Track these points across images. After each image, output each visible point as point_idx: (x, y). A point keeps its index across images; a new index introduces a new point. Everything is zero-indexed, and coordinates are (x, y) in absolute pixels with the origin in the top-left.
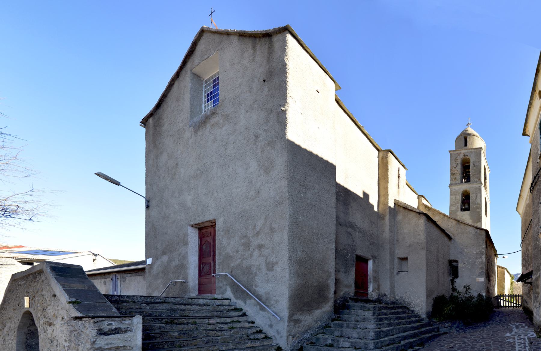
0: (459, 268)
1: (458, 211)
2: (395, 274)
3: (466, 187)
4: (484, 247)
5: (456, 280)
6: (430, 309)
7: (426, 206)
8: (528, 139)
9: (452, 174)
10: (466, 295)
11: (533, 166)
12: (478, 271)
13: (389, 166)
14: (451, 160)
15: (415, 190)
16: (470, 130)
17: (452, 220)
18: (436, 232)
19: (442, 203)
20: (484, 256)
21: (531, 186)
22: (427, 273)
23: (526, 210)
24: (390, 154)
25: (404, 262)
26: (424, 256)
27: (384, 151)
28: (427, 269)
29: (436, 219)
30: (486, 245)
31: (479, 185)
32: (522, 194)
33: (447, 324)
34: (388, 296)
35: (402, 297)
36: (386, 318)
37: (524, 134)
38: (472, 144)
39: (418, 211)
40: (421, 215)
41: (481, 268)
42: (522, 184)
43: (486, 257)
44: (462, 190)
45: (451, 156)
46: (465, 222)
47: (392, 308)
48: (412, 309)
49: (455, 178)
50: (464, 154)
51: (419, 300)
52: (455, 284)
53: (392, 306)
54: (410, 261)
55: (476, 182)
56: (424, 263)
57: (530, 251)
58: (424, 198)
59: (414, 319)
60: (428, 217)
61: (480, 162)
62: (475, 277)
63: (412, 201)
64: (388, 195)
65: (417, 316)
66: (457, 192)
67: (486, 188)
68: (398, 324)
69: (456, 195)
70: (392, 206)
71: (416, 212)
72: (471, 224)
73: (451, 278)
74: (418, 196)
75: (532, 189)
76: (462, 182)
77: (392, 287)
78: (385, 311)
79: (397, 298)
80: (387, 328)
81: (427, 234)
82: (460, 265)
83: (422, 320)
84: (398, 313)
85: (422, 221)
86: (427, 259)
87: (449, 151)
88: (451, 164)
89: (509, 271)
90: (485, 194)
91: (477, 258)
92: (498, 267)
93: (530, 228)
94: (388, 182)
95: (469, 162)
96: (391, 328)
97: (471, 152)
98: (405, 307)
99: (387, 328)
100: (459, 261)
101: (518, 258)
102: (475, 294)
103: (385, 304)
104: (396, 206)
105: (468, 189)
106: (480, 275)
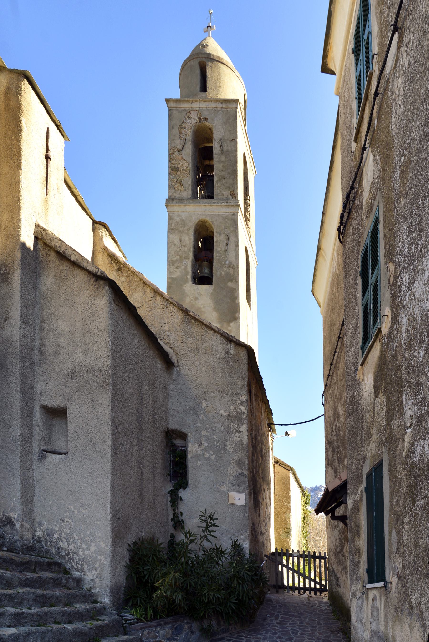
0: (189, 456)
1: (186, 281)
2: (35, 456)
3: (200, 211)
4: (244, 398)
5: (182, 493)
6: (122, 579)
7: (112, 257)
8: (331, 81)
9: (173, 169)
10: (206, 544)
11: (343, 161)
12: (232, 471)
13: (23, 119)
14: (171, 127)
15: (87, 205)
16: (214, 48)
17: (173, 309)
18: (136, 340)
19: (152, 259)
20: (244, 427)
21: (341, 223)
22: (113, 462)
23: (331, 293)
24: (26, 86)
25: (57, 423)
26: (108, 411)
27: (12, 71)
28: (115, 453)
29: (135, 298)
30: (250, 392)
31: (232, 210)
32: (323, 246)
33: (162, 632)
34: (18, 525)
35: (51, 534)
36: (10, 598)
37: (326, 69)
38: (218, 87)
39: (92, 269)
40: (102, 283)
41: (239, 463)
42: (323, 214)
43: (250, 430)
44: (195, 220)
45: (170, 115)
46: (202, 317)
47: (25, 566)
48: (77, 574)
49: (180, 182)
50: (199, 112)
51: (93, 548)
52: (182, 508)
53: (26, 558)
54: (73, 423)
55: (226, 200)
56: (107, 431)
57: (342, 419)
58: (108, 230)
59: (81, 607)
60: (114, 288)
61: (234, 140)
62: (224, 488)
63: (79, 238)
64: (19, 207)
65: (89, 597)
66: (183, 223)
67: (247, 220)
68: (41, 620)
69: (181, 233)
70: (30, 244)
71: (90, 273)
72: (216, 325)
73: (170, 487)
74: (95, 222)
75: (342, 232)
76: (194, 196)
77: (28, 499)
78: (8, 574)
79: (39, 534)
80: (12, 631)
81: (114, 344)
82: (192, 449)
83: (102, 611)
84: (40, 583)
85: (103, 302)
86: (113, 421)
87: (167, 100)
88: (171, 139)
89: (299, 476)
90: (246, 239)
91: (228, 431)
92: (277, 462)
93: (341, 349)
94: (19, 167)
95: (210, 139)
96: (23, 629)
97: (216, 110)
98: (59, 565)
99: (12, 631)
100: (191, 437)
101: (316, 437)
102: (226, 544)
103: (10, 550)
104: (40, 245)
105: (208, 219)
106: (236, 485)
